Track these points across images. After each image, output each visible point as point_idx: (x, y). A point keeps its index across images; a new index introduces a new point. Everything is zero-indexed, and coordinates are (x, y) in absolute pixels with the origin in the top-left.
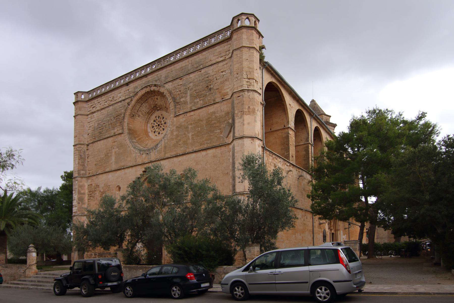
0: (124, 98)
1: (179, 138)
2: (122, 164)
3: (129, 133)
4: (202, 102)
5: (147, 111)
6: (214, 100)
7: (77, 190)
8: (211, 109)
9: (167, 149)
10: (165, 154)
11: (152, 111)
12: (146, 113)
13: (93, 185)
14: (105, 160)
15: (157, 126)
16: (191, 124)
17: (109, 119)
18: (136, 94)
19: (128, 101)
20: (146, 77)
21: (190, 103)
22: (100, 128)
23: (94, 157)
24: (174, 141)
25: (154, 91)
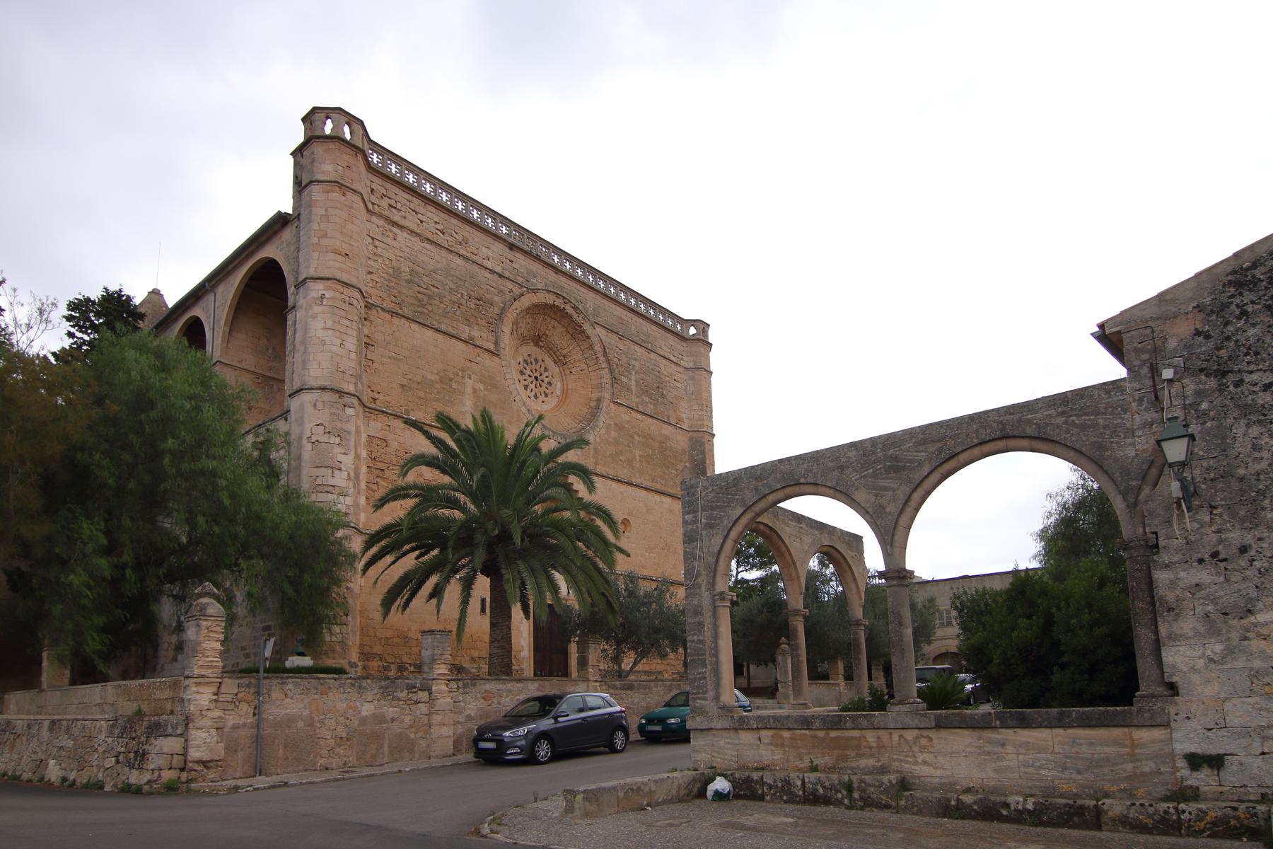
0: (499, 270)
5: (526, 333)
14: (438, 392)
17: (452, 286)
18: (535, 291)
20: (556, 273)
22: (422, 290)
25: (571, 317)
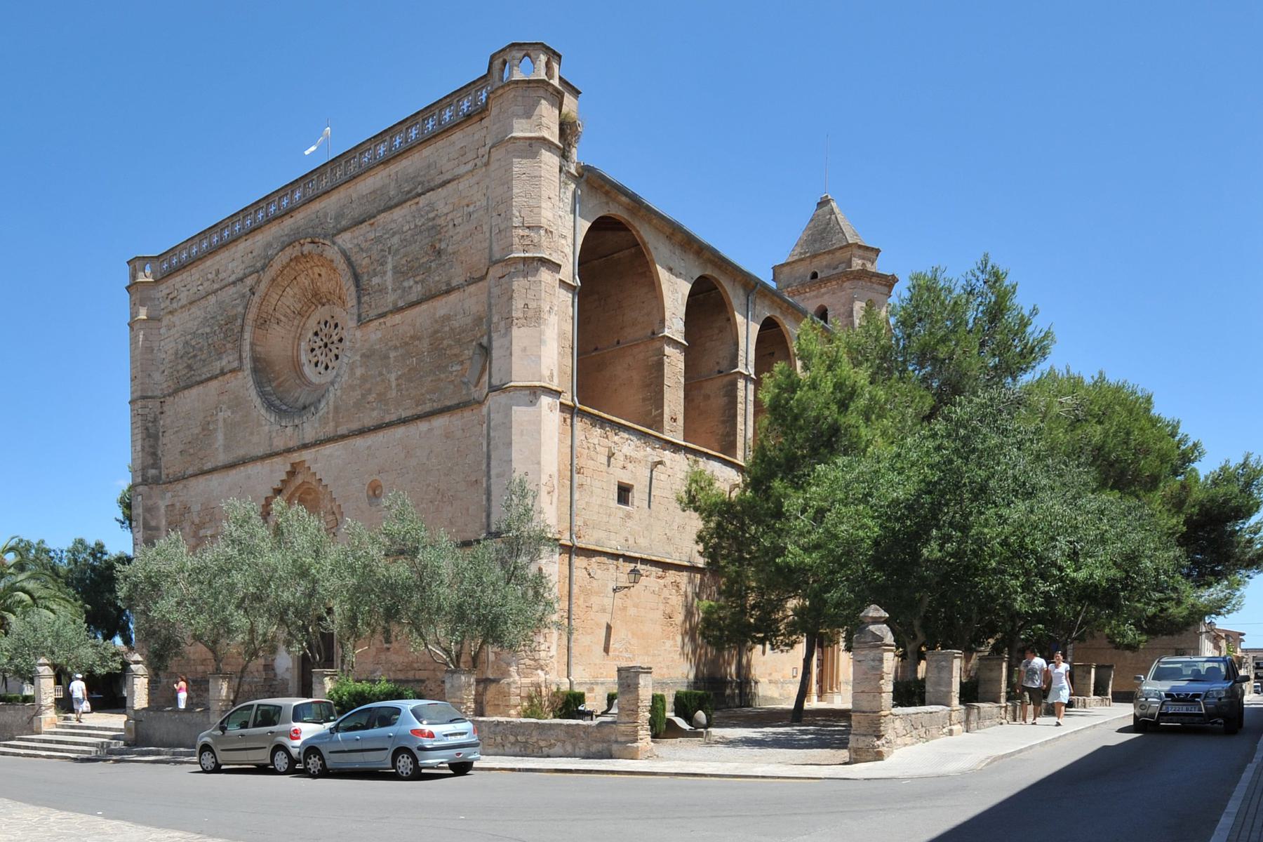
1: (368, 386)
2: (241, 452)
3: (255, 371)
4: (419, 286)
6: (448, 284)
7: (141, 518)
8: (442, 307)
9: (341, 415)
10: (337, 426)
11: (310, 307)
12: (294, 312)
13: (178, 505)
15: (323, 348)
16: (396, 348)
17: (208, 330)
19: (249, 281)
21: (394, 290)
23: (177, 432)
24: (357, 394)
